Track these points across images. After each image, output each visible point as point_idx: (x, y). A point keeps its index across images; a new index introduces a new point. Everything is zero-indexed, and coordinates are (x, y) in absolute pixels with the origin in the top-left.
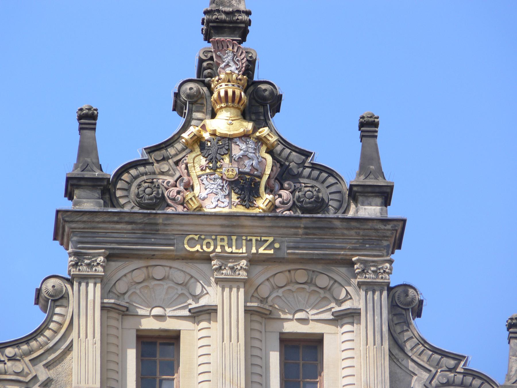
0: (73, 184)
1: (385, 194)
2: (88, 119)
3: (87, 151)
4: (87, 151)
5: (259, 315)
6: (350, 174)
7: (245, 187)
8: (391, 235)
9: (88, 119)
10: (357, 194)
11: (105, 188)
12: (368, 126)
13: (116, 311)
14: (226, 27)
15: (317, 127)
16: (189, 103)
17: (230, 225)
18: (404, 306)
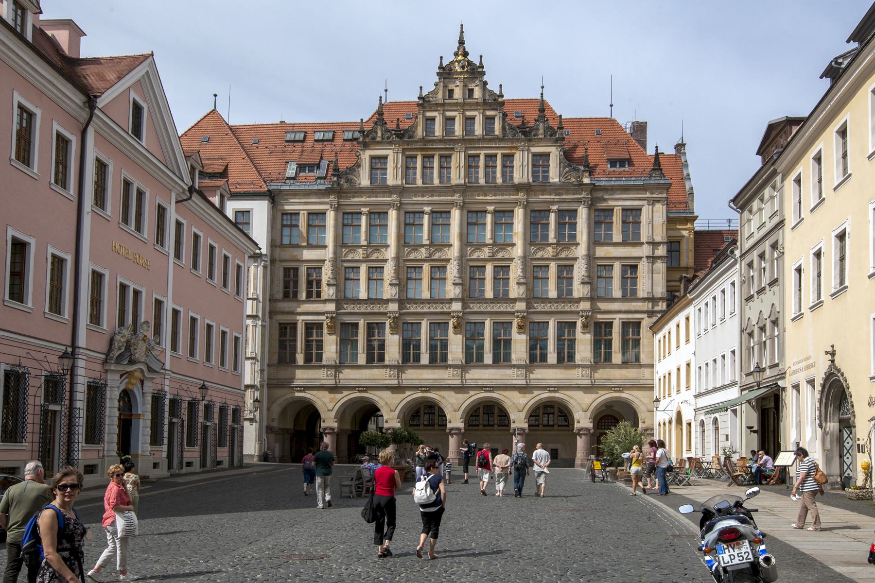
0: (439, 68)
1: (483, 67)
2: (441, 58)
3: (441, 63)
4: (441, 63)
5: (465, 86)
6: (478, 64)
7: (463, 67)
8: (484, 73)
9: (441, 58)
10: (479, 67)
11: (444, 68)
12: (481, 57)
13: (445, 86)
14: (461, 42)
15: (474, 58)
16: (456, 54)
17: (461, 73)
18: (485, 83)
